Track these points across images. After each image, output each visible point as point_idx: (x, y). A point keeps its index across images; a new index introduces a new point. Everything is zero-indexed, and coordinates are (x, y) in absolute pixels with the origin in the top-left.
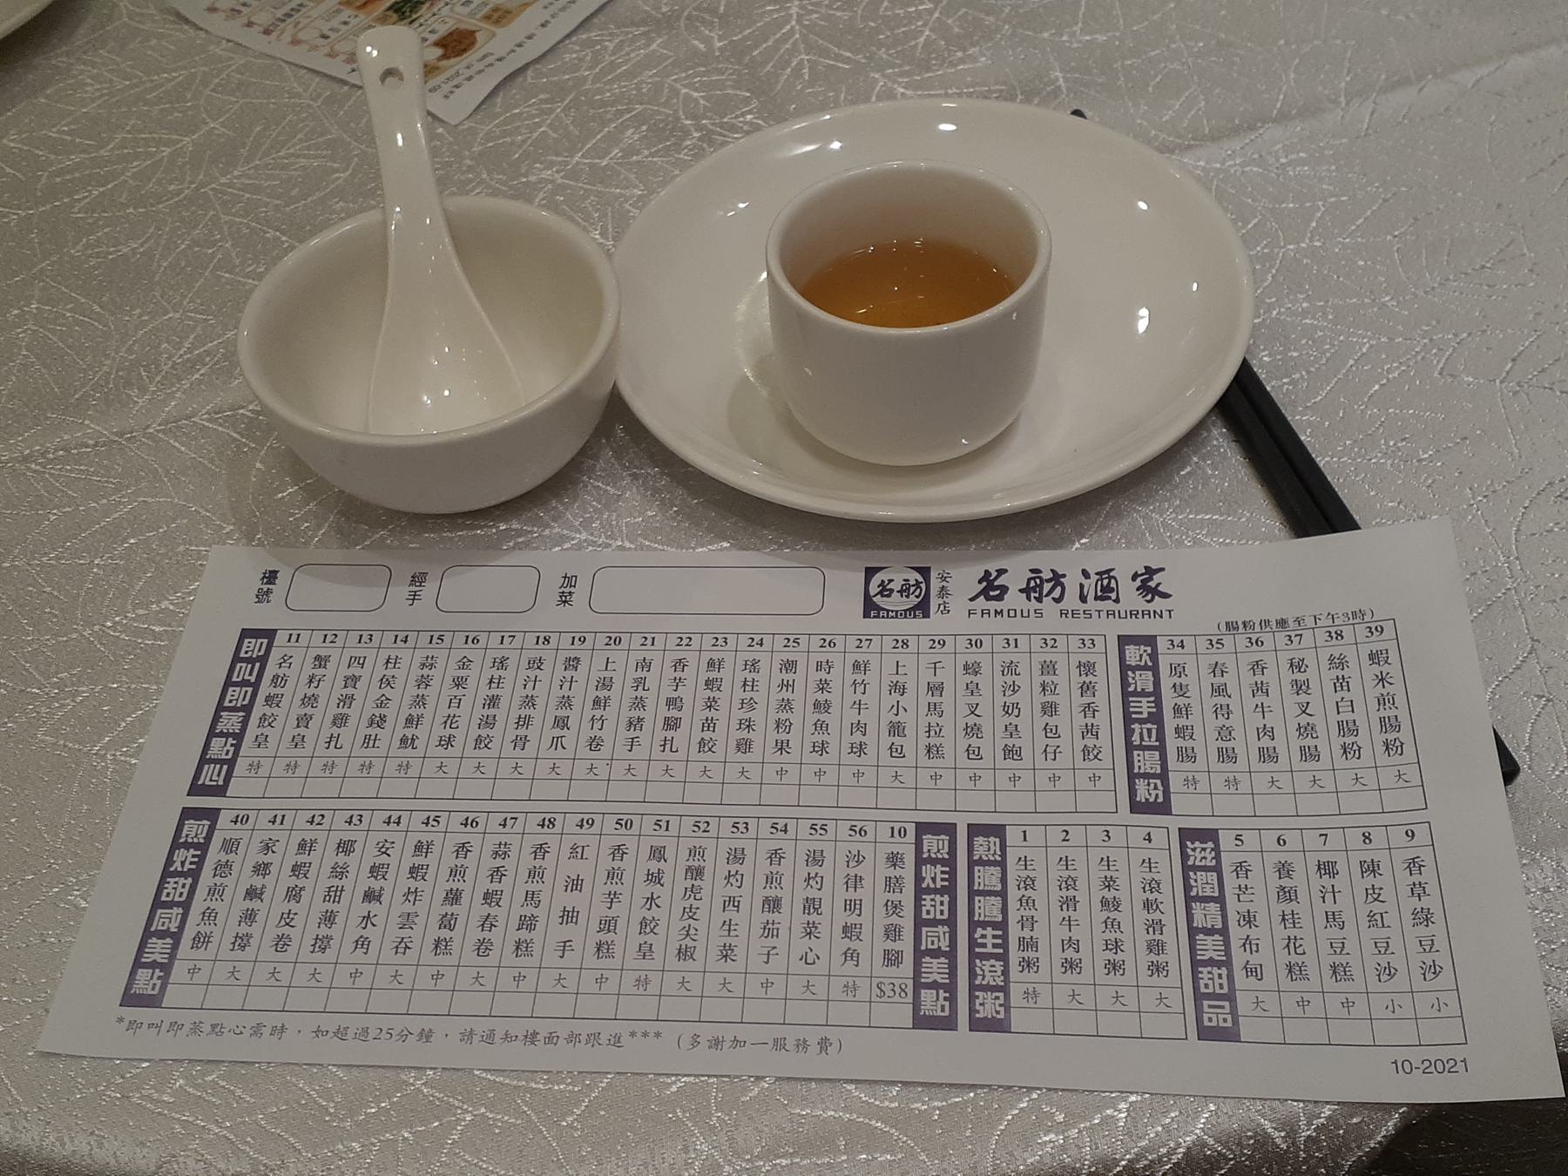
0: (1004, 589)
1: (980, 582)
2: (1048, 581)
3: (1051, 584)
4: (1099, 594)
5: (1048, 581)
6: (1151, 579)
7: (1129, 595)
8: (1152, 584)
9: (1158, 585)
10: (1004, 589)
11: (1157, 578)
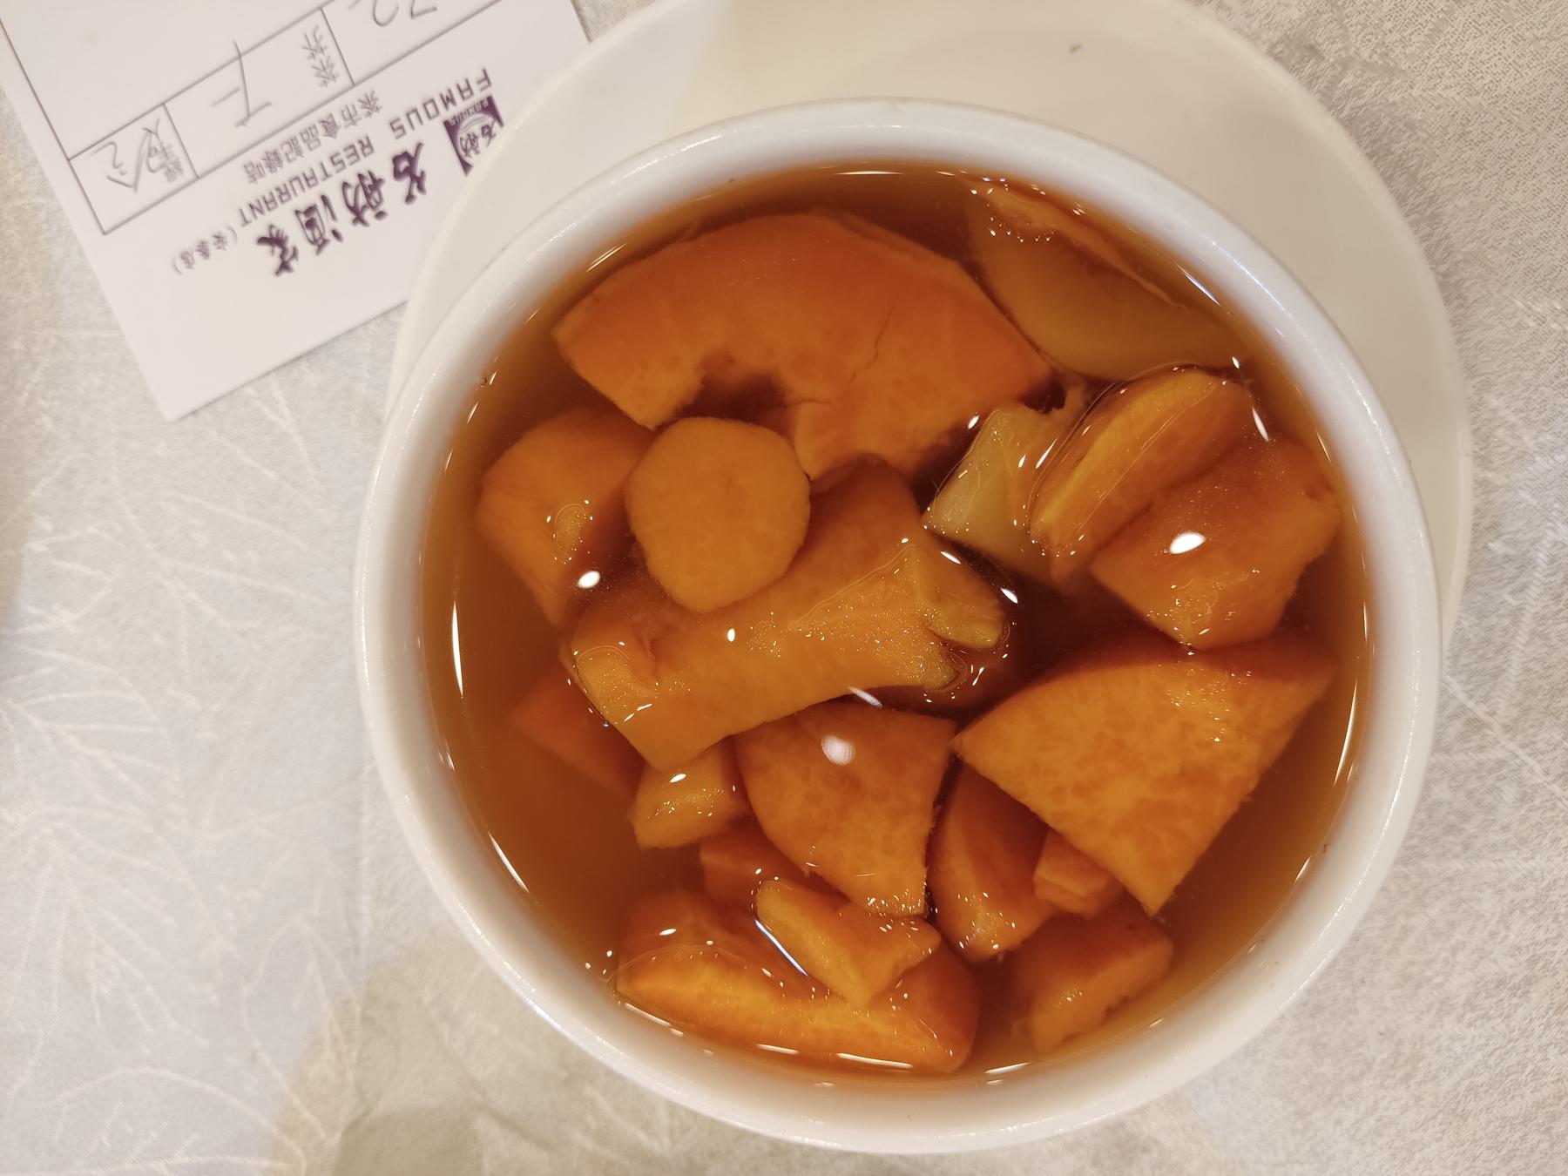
0: (397, 174)
6: (282, 256)
7: (285, 220)
9: (273, 252)
10: (397, 174)
11: (275, 261)
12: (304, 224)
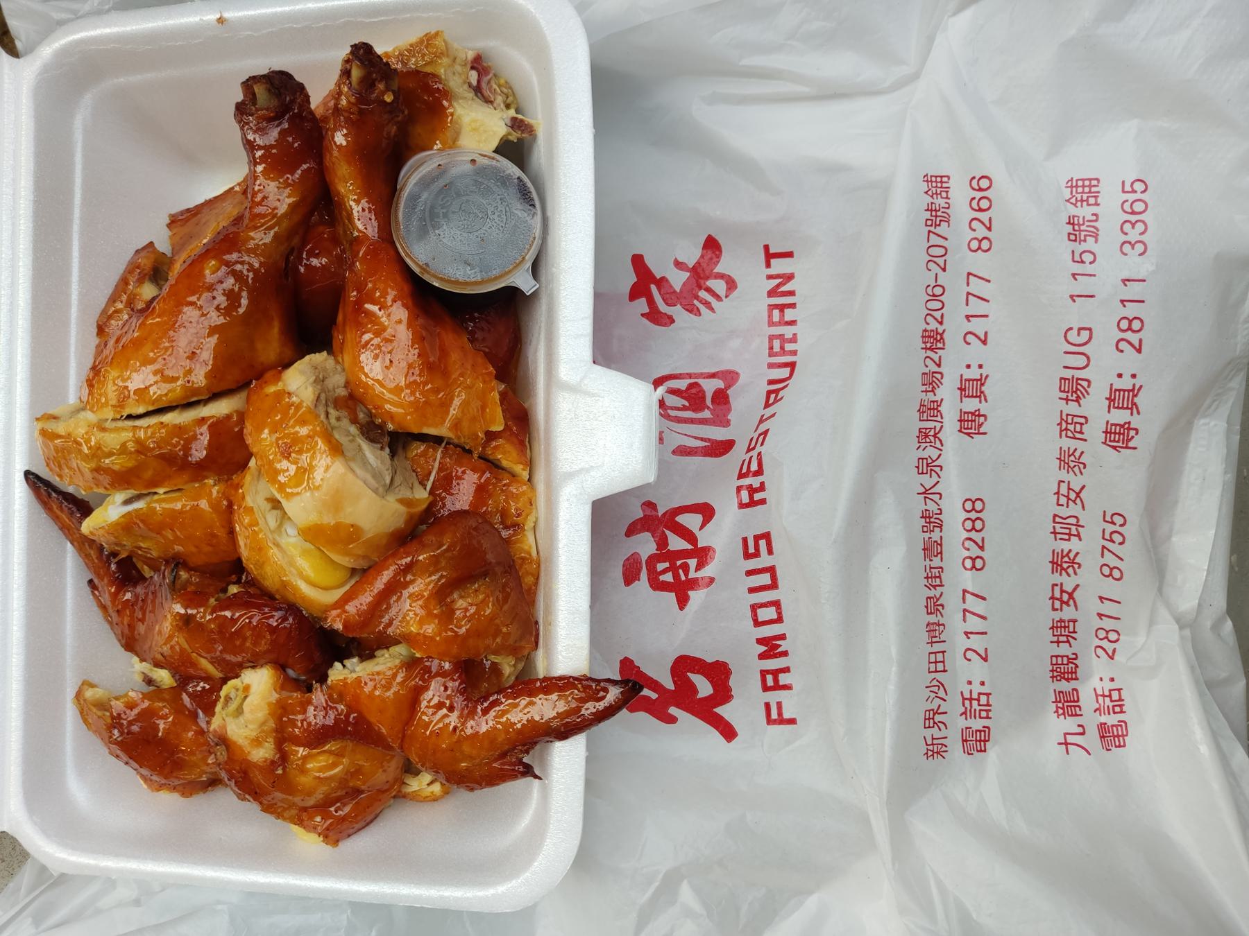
1: (672, 720)
2: (662, 542)
3: (668, 533)
4: (706, 414)
5: (662, 542)
8: (678, 279)
9: (678, 264)
12: (701, 381)
